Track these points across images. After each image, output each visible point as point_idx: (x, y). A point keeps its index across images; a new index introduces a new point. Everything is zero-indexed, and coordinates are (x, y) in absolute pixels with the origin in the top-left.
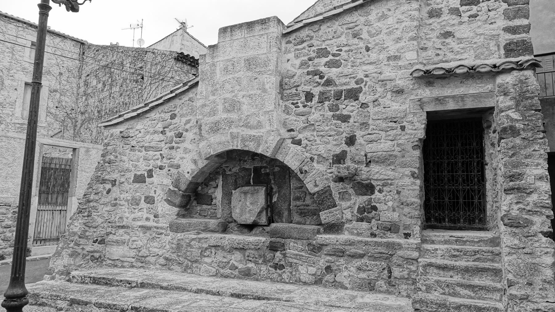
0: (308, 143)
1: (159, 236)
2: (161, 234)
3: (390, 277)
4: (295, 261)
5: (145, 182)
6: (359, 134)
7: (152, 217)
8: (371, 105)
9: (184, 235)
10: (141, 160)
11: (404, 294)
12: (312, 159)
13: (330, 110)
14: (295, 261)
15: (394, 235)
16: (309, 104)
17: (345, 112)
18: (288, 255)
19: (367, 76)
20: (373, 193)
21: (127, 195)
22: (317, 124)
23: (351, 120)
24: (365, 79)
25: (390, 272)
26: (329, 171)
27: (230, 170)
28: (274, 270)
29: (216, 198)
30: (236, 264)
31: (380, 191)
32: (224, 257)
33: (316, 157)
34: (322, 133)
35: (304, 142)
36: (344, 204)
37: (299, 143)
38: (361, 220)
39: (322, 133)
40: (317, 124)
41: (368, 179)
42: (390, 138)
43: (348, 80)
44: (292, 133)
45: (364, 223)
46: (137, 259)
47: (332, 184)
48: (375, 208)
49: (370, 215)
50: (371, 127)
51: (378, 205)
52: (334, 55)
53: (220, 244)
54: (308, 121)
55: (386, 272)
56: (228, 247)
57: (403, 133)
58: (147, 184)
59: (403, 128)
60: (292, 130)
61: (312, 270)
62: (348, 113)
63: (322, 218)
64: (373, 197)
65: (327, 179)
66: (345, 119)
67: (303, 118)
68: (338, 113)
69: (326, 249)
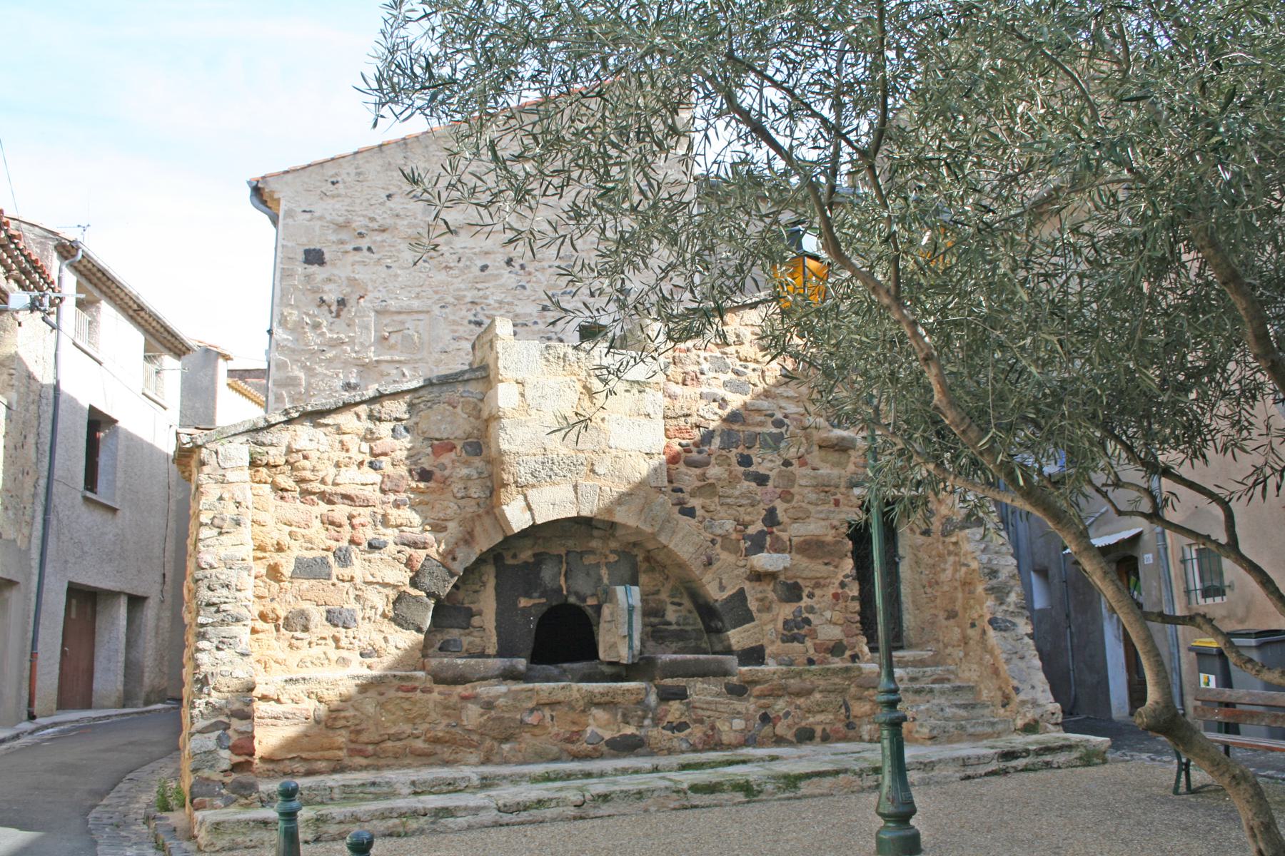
0: (706, 514)
1: (410, 695)
2: (414, 689)
3: (848, 717)
4: (709, 713)
5: (329, 577)
6: (780, 507)
7: (354, 657)
8: (795, 462)
9: (474, 688)
10: (317, 523)
11: (866, 737)
12: (713, 541)
13: (740, 463)
14: (709, 713)
15: (837, 659)
16: (706, 448)
17: (762, 471)
18: (697, 705)
19: (786, 417)
20: (800, 598)
21: (275, 605)
22: (721, 484)
23: (770, 483)
24: (786, 421)
25: (847, 709)
26: (742, 563)
27: (515, 556)
28: (669, 733)
29: (480, 613)
30: (600, 731)
31: (811, 596)
32: (574, 723)
33: (719, 539)
34: (729, 500)
35: (699, 512)
36: (766, 616)
37: (690, 512)
38: (794, 639)
39: (729, 500)
40: (721, 484)
41: (795, 577)
42: (822, 516)
43: (763, 418)
44: (681, 495)
45: (796, 644)
46: (349, 750)
47: (747, 586)
48: (807, 621)
49: (803, 632)
50: (797, 498)
51: (810, 616)
52: (737, 373)
53: (562, 699)
54: (703, 477)
55: (843, 710)
56: (581, 703)
57: (837, 509)
58: (334, 580)
59: (837, 503)
60: (681, 490)
61: (739, 724)
62: (767, 473)
63: (733, 641)
64: (802, 604)
65: (738, 576)
66: (762, 480)
67: (698, 471)
68: (751, 469)
69: (757, 689)
